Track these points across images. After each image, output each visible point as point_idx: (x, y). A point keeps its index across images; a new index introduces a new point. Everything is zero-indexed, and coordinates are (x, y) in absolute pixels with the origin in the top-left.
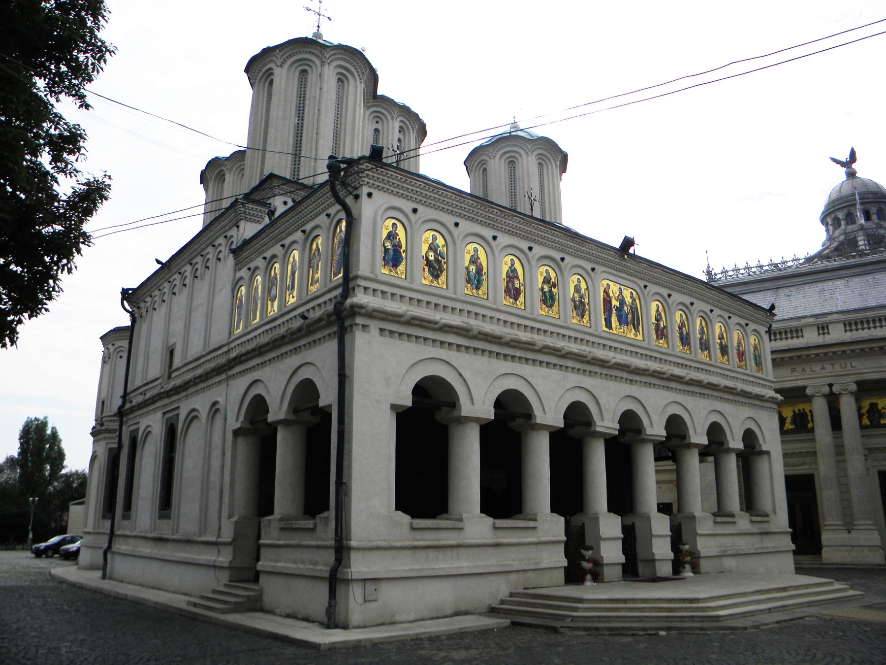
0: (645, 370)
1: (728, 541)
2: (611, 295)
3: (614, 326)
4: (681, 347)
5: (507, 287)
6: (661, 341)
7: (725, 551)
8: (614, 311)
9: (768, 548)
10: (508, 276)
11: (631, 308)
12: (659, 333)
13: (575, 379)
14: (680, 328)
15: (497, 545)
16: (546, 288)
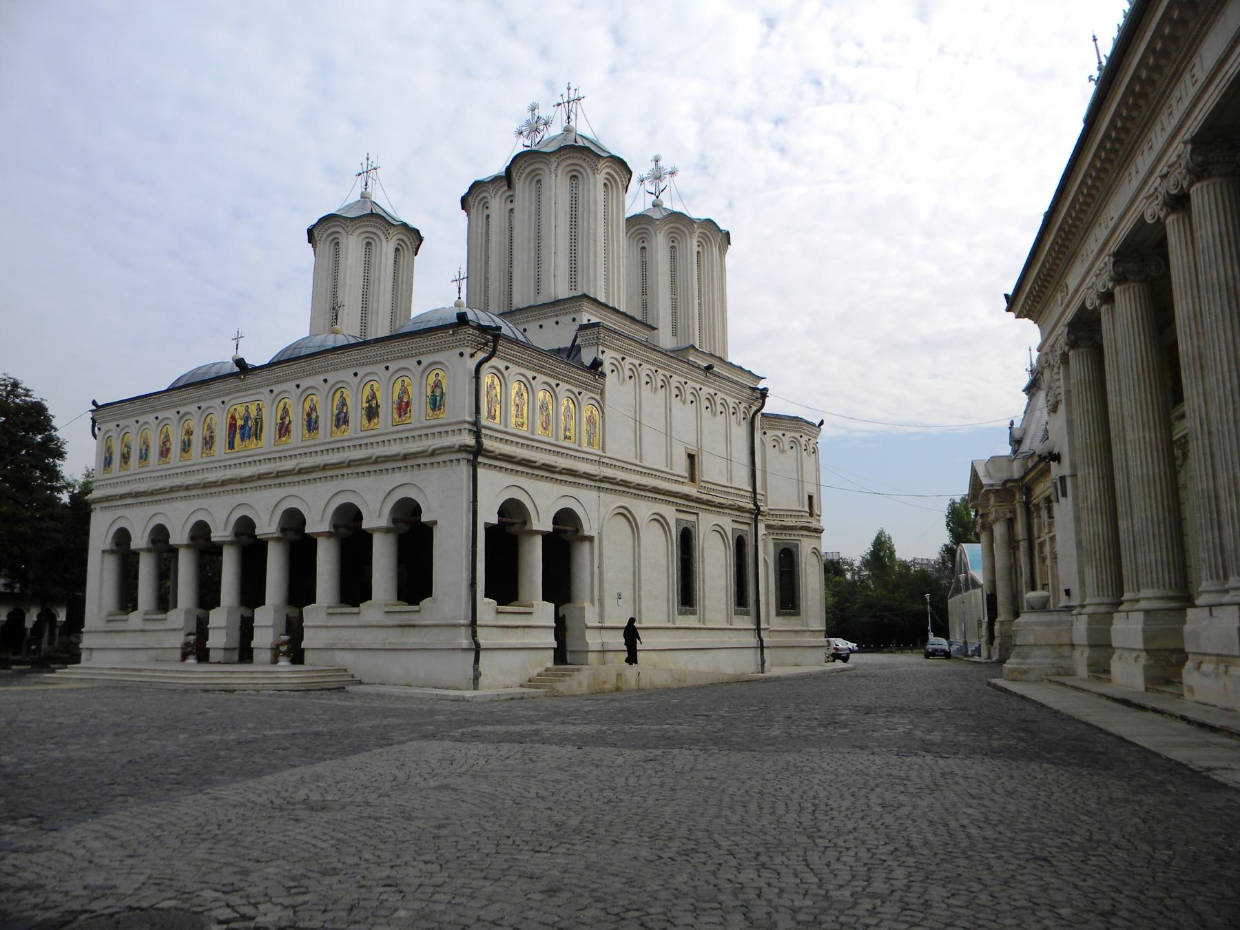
0: (250, 477)
1: (345, 634)
2: (237, 417)
3: (236, 444)
4: (307, 435)
5: (162, 451)
6: (284, 439)
7: (335, 644)
8: (238, 431)
9: (405, 643)
10: (164, 443)
11: (256, 419)
12: (283, 431)
13: (195, 504)
14: (309, 415)
15: (142, 631)
16: (186, 438)
